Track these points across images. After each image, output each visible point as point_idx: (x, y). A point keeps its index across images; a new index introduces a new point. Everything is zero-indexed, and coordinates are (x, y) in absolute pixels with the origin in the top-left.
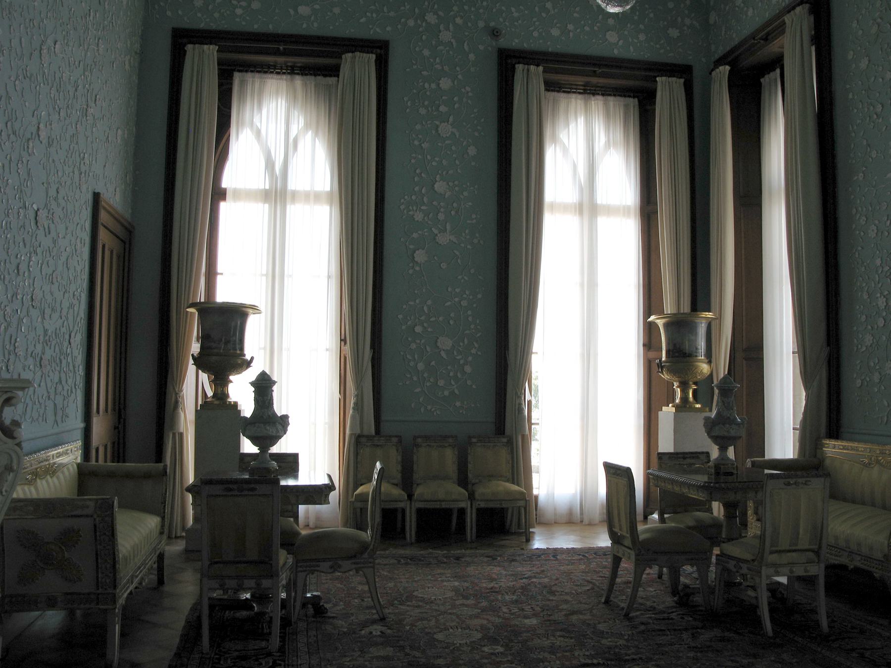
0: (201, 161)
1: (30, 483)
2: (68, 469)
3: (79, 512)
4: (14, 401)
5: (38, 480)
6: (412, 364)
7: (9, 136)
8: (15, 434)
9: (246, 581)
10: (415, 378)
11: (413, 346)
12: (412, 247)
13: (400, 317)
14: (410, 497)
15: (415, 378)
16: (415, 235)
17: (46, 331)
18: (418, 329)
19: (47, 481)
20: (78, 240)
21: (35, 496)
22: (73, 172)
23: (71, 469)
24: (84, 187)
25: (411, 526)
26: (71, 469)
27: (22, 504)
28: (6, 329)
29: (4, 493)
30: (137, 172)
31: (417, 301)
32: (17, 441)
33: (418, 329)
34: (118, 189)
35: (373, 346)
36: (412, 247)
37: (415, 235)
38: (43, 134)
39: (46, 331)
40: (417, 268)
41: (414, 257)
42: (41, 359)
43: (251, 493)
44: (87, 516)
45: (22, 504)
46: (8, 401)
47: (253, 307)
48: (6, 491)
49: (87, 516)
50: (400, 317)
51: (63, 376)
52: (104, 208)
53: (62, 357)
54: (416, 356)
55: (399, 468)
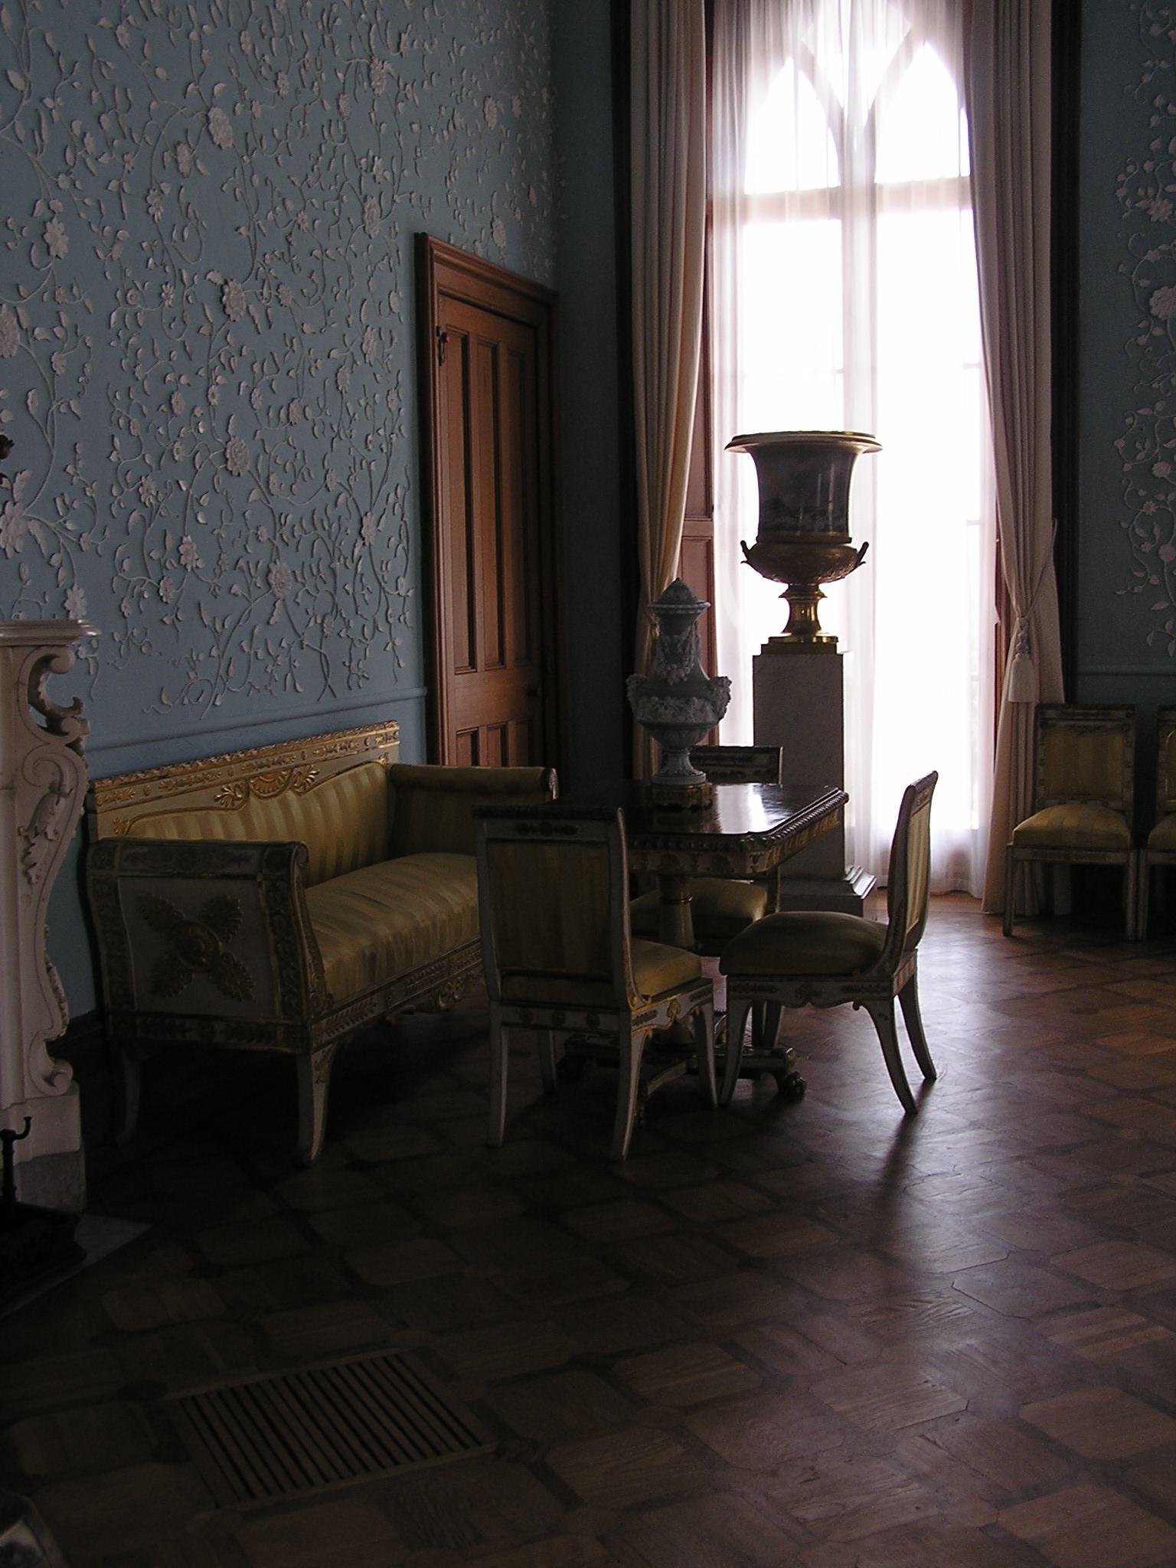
0: (677, 144)
1: (229, 805)
2: (355, 779)
3: (234, 869)
4: (54, 663)
5: (253, 799)
6: (1147, 547)
7: (109, 144)
8: (65, 725)
9: (602, 1018)
10: (1154, 580)
11: (1151, 508)
12: (1144, 283)
13: (1120, 444)
14: (1140, 839)
15: (1154, 580)
16: (1151, 256)
17: (277, 520)
18: (1161, 470)
19: (285, 807)
20: (371, 335)
21: (240, 835)
22: (339, 198)
23: (365, 780)
24: (376, 229)
25: (1136, 903)
26: (365, 780)
27: (145, 850)
28: (145, 523)
29: (50, 835)
30: (563, 183)
31: (1159, 406)
32: (70, 739)
33: (1161, 470)
34: (498, 222)
35: (1057, 513)
36: (1144, 283)
37: (1151, 256)
38: (223, 130)
39: (277, 520)
40: (1158, 332)
41: (1149, 308)
42: (269, 571)
43: (567, 838)
44: (244, 877)
45: (145, 850)
46: (45, 663)
47: (860, 438)
48: (56, 833)
49: (244, 877)
50: (1120, 444)
51: (343, 600)
52: (442, 261)
53: (337, 565)
54: (1156, 530)
55: (1129, 774)
